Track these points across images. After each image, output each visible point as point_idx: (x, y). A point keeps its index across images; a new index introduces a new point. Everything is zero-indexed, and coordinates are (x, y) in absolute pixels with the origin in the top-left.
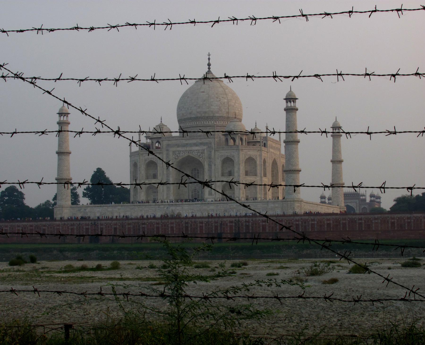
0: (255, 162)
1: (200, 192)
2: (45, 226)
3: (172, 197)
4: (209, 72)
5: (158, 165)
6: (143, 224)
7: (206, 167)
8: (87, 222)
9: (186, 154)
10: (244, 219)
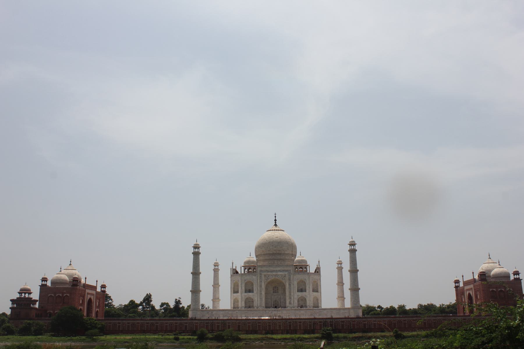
2: (186, 323)
3: (264, 305)
4: (276, 225)
6: (259, 323)
8: (218, 321)
10: (329, 320)
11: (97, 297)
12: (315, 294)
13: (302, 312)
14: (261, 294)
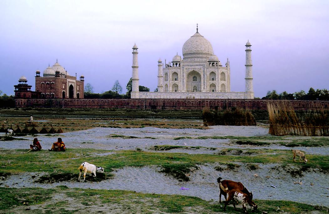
0: (225, 75)
1: (197, 87)
3: (185, 89)
4: (197, 32)
5: (178, 74)
7: (202, 76)
9: (193, 70)
11: (77, 85)
12: (223, 82)
13: (210, 94)
14: (183, 82)
